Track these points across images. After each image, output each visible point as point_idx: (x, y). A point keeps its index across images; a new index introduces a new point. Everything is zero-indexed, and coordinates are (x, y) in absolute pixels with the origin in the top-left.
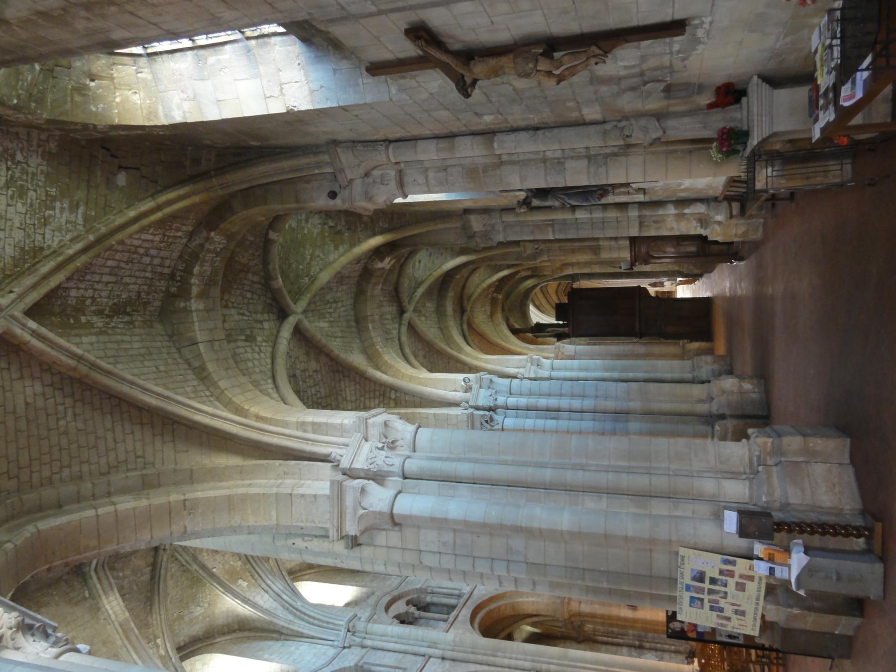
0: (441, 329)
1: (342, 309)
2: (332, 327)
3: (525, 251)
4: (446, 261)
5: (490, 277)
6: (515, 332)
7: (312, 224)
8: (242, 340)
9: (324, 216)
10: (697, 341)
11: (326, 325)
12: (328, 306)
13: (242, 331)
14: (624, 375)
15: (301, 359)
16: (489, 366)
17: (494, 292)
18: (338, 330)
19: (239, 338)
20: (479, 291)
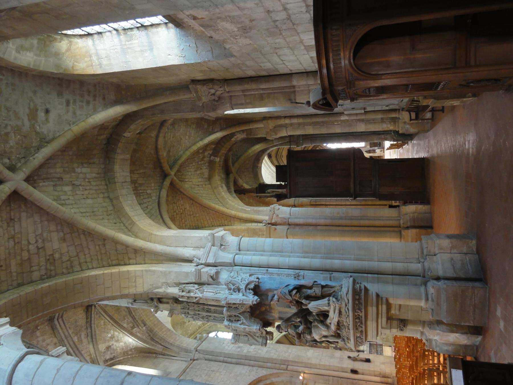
0: (111, 200)
3: (200, 99)
4: (95, 111)
5: (202, 139)
6: (240, 192)
10: (411, 203)
14: (328, 263)
16: (159, 248)
17: (211, 155)
20: (188, 153)
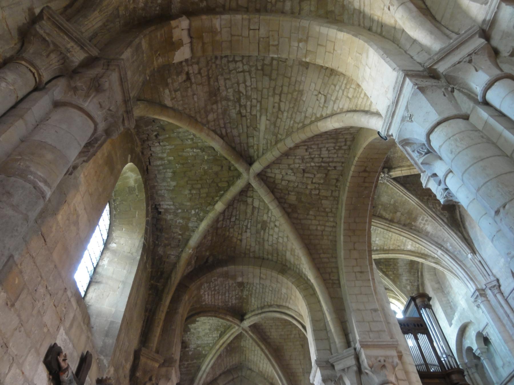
1: (248, 83)
2: (267, 110)
7: (163, 153)
8: (264, 233)
9: (150, 143)
11: (264, 118)
12: (243, 112)
13: (258, 232)
15: (291, 162)
18: (271, 99)
19: (262, 237)
